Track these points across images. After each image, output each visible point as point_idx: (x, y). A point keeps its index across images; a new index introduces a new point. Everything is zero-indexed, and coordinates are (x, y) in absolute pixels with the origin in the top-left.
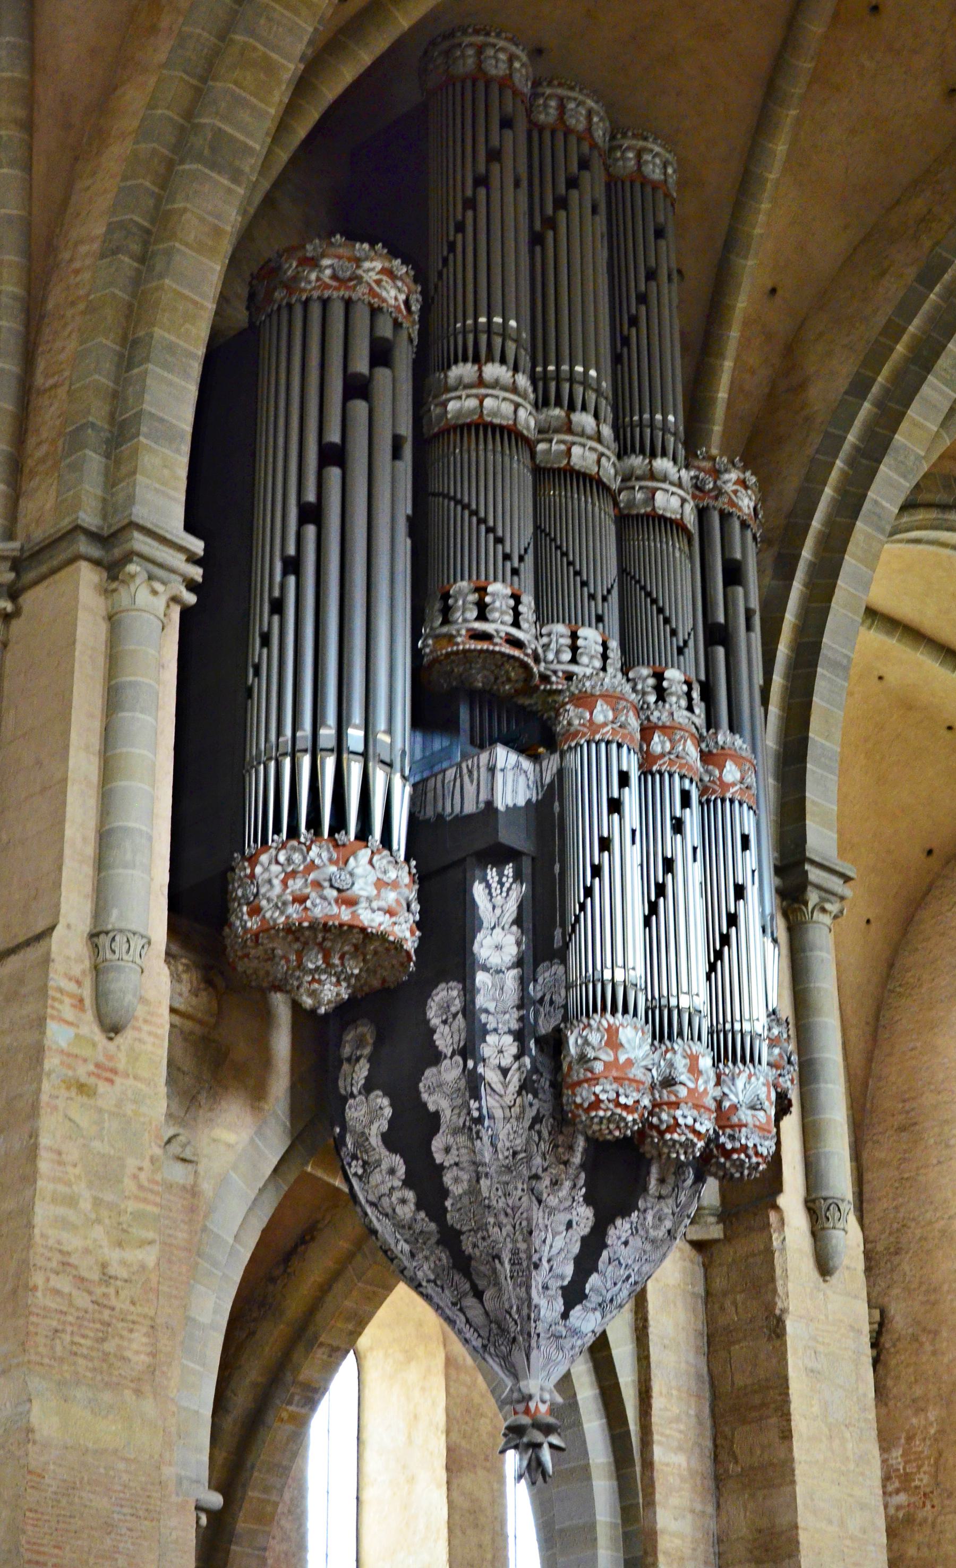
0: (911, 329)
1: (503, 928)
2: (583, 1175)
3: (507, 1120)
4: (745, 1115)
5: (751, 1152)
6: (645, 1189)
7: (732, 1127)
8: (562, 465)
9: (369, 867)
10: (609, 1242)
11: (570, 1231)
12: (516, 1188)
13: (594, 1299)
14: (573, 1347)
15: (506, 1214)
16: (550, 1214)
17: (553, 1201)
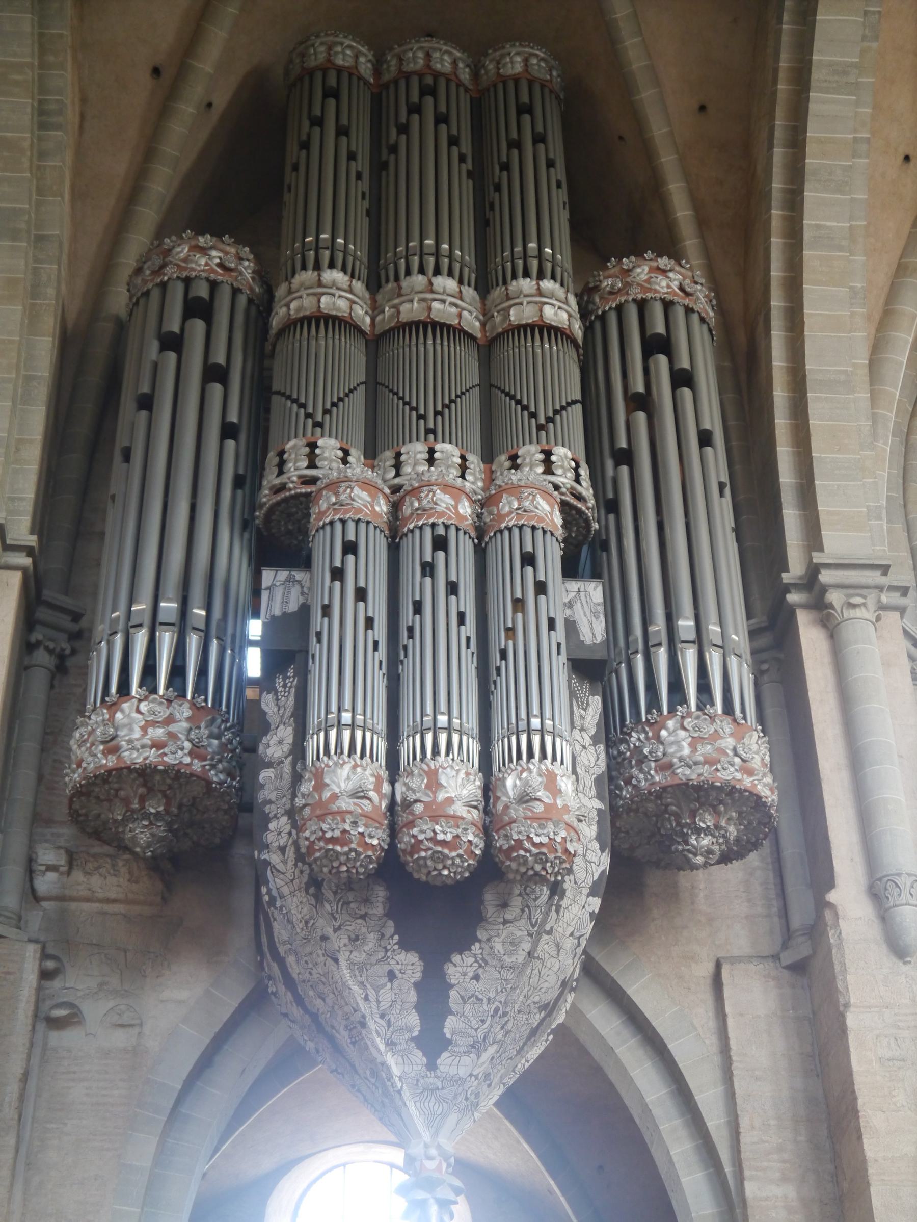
0: (783, 64)
1: (284, 724)
2: (391, 923)
3: (292, 893)
4: (517, 812)
5: (527, 845)
6: (479, 918)
7: (503, 827)
8: (393, 325)
9: (135, 715)
10: (453, 981)
11: (396, 983)
12: (318, 956)
13: (462, 1043)
14: (455, 1097)
15: (324, 984)
16: (361, 970)
17: (359, 957)
